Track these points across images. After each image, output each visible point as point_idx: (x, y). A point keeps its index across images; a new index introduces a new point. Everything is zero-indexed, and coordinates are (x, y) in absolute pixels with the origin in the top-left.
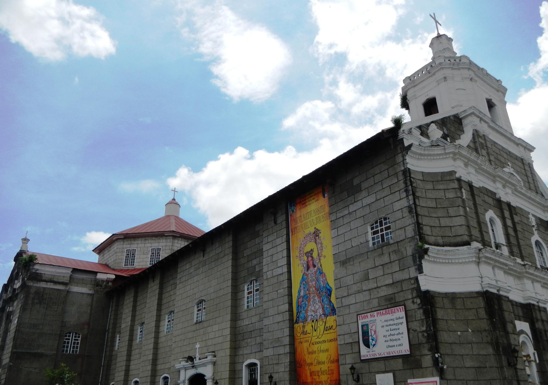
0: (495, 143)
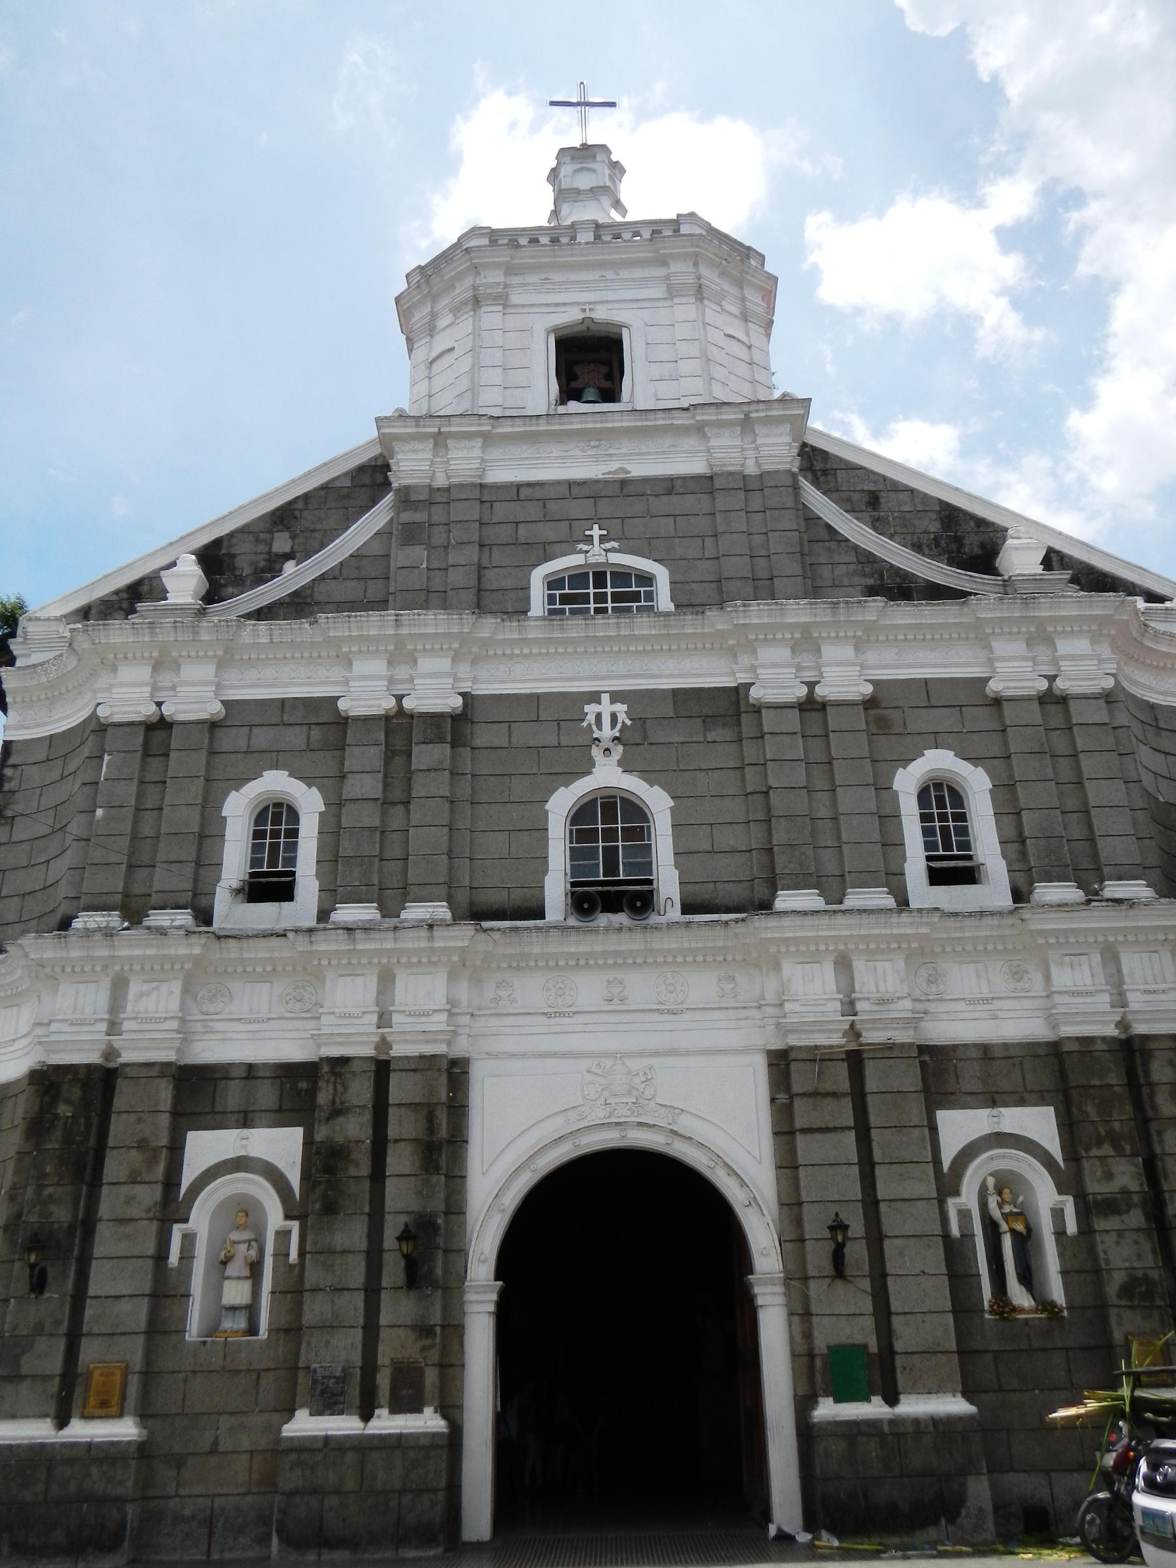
0: (519, 486)
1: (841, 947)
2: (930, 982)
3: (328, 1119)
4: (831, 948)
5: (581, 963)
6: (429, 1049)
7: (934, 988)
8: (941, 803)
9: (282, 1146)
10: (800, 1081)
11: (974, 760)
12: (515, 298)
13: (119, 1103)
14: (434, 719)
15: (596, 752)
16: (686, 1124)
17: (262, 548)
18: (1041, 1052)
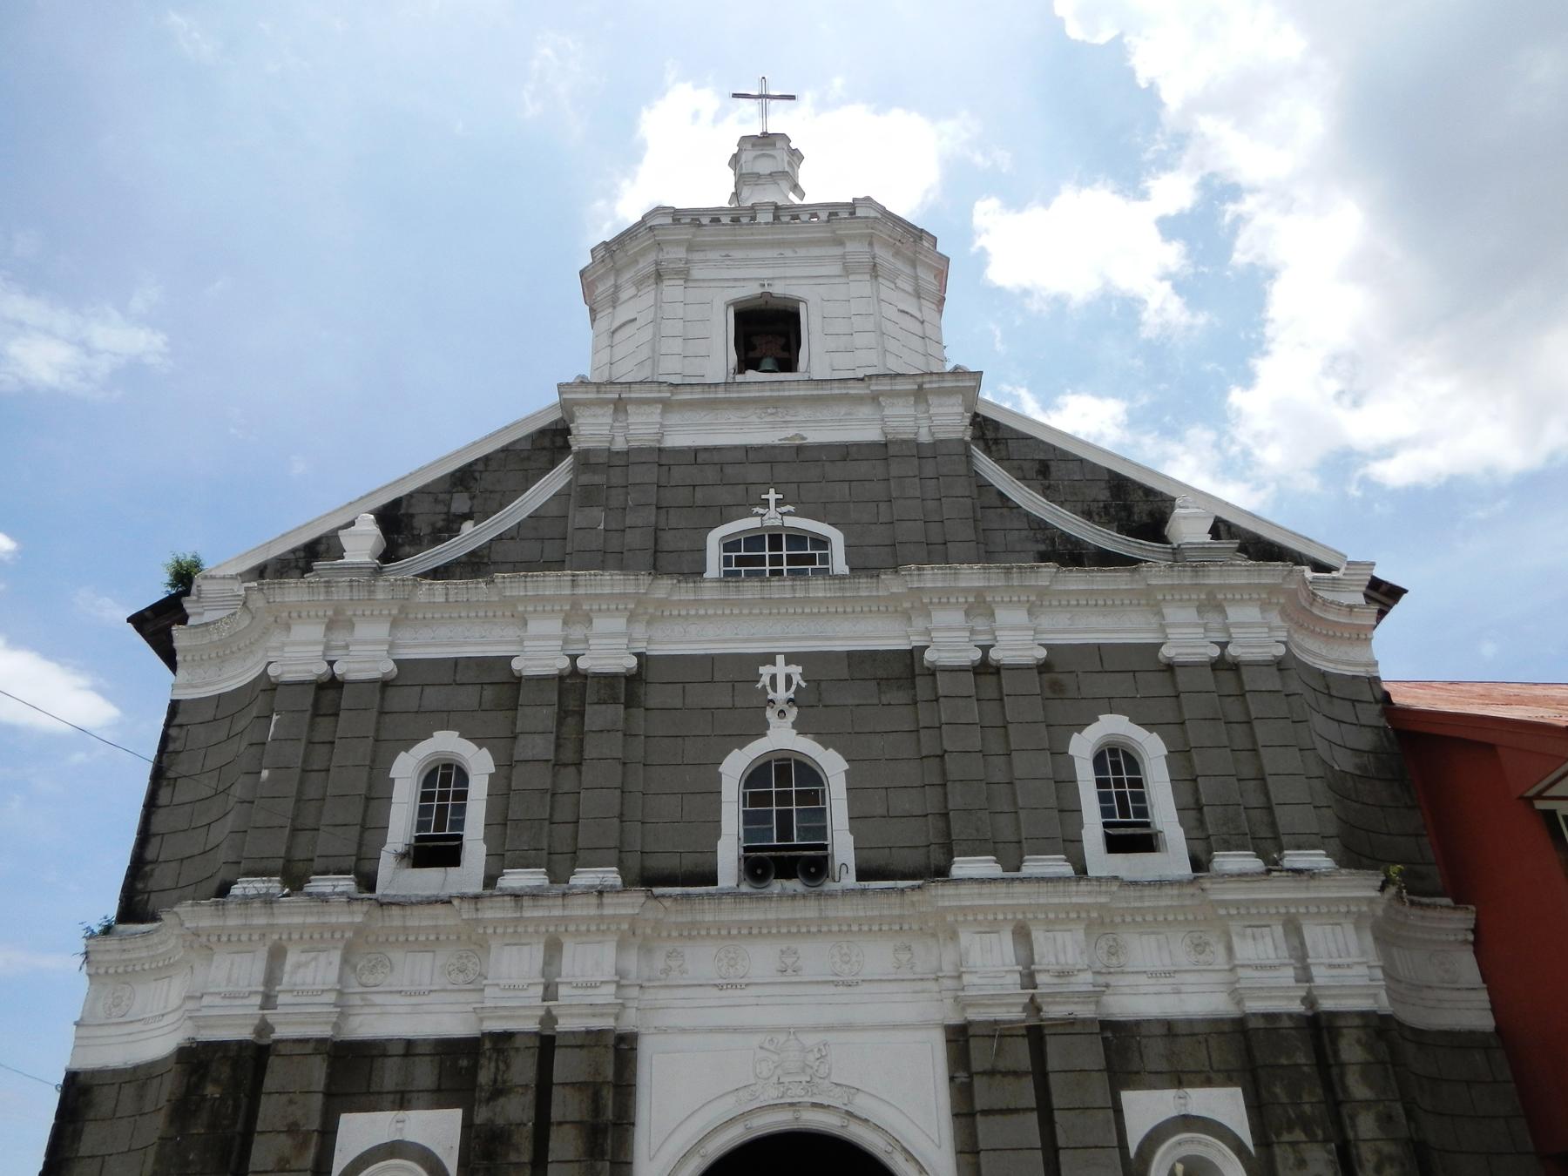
1: (1020, 916)
2: (1112, 953)
3: (489, 1100)
4: (1010, 917)
5: (754, 932)
6: (597, 1024)
7: (1114, 961)
8: (1117, 769)
9: (439, 1129)
10: (980, 1057)
11: (1149, 726)
12: (696, 273)
13: (269, 1083)
14: (608, 680)
15: (771, 714)
16: (862, 1105)
17: (441, 508)
18: (1226, 1028)
